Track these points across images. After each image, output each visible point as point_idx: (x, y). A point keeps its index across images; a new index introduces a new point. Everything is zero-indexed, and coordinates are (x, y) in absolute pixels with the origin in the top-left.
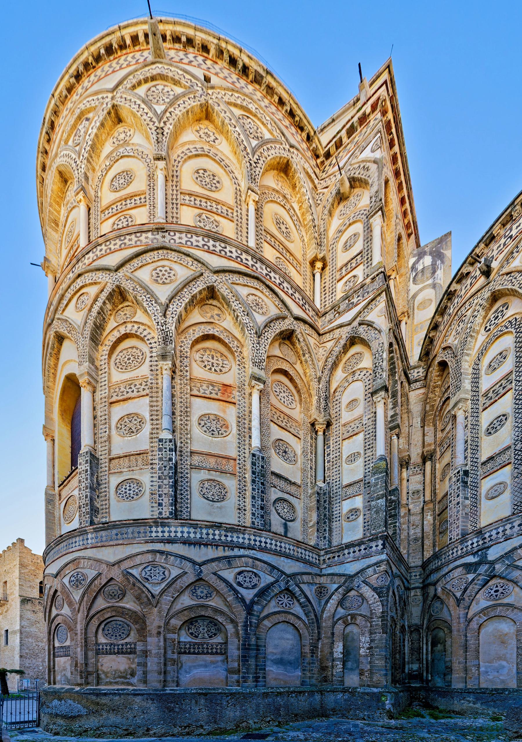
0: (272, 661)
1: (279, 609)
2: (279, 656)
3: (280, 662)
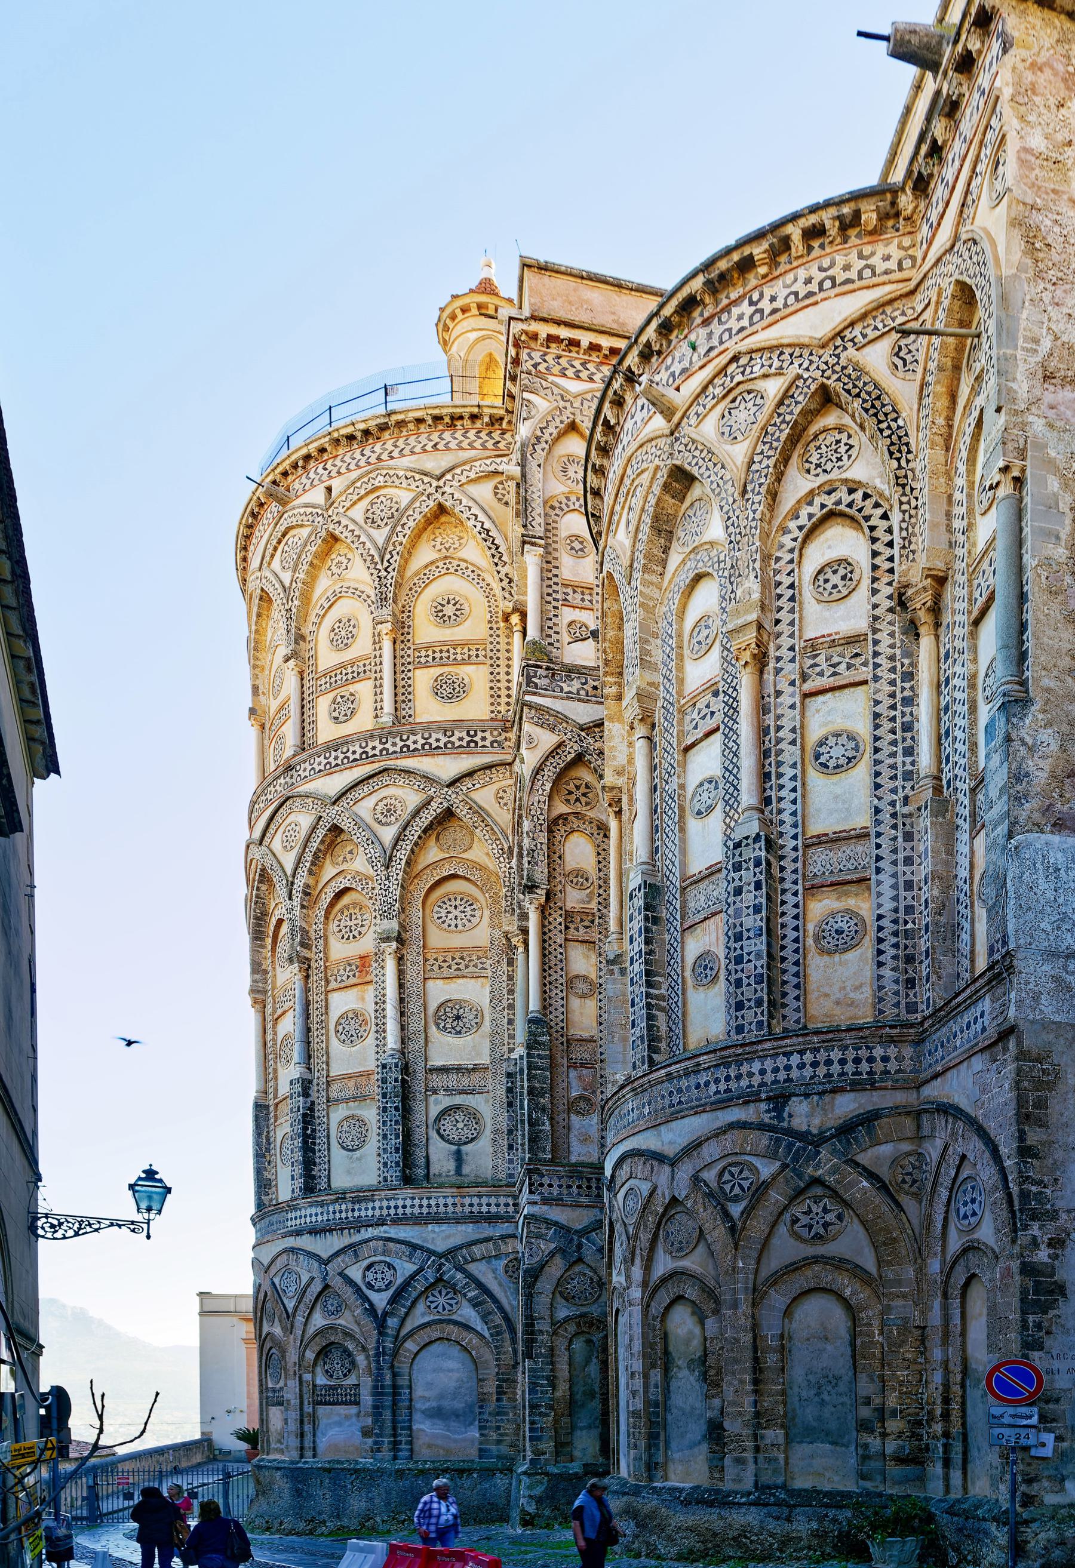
0: (423, 1412)
1: (432, 1318)
2: (434, 1404)
3: (437, 1413)
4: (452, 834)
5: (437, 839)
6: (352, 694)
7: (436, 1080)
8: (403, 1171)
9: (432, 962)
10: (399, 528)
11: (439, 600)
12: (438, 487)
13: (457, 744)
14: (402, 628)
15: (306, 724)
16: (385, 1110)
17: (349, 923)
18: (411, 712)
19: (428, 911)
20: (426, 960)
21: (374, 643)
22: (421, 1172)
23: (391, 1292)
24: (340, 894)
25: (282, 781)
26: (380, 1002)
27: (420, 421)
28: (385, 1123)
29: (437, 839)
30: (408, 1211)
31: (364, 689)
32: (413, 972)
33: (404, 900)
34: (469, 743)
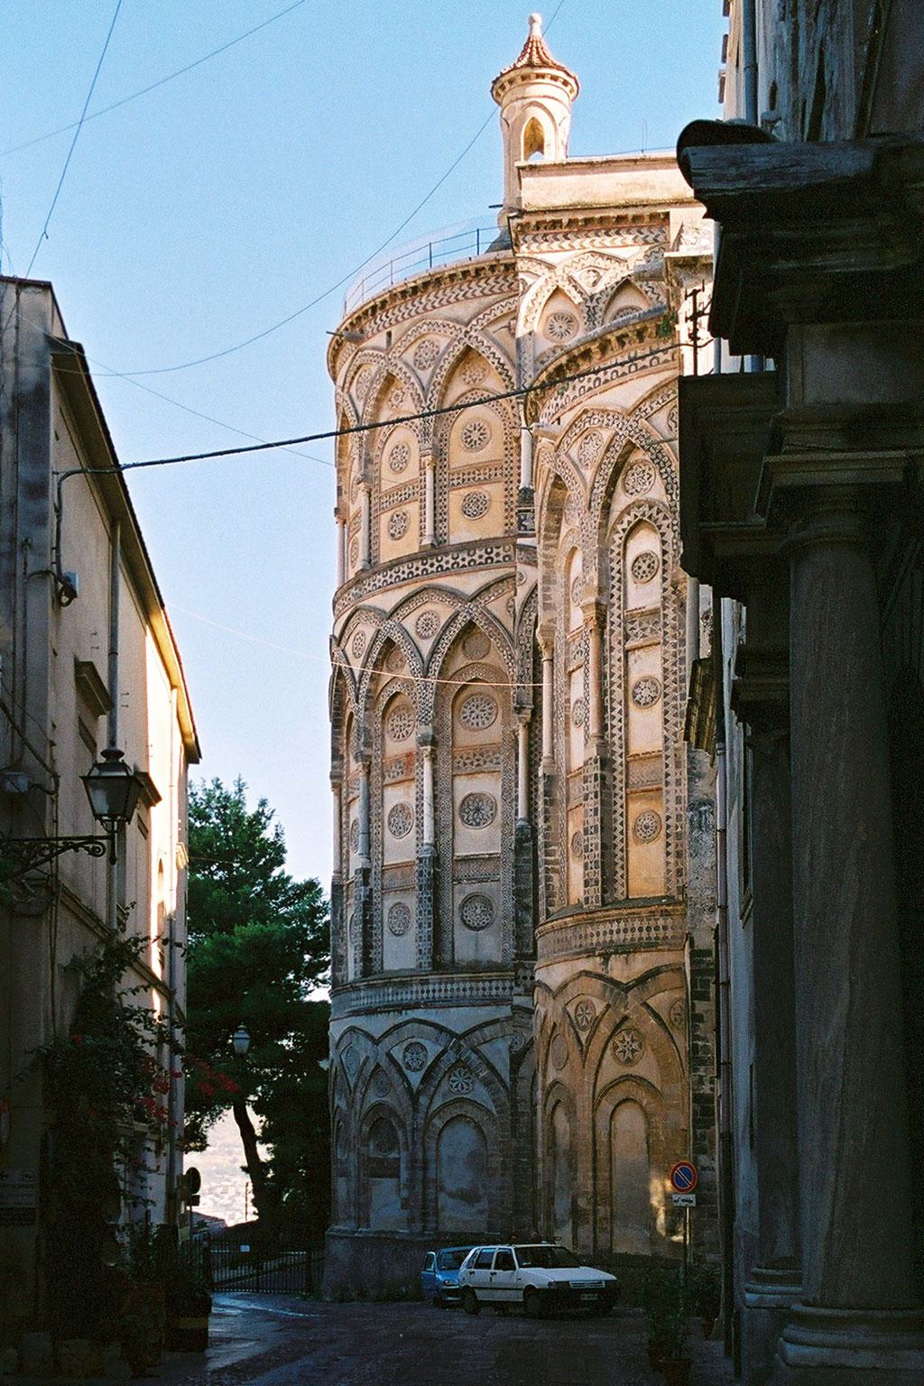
4: (473, 642)
5: (464, 647)
6: (404, 514)
7: (462, 870)
8: (433, 958)
9: (458, 759)
10: (438, 371)
11: (468, 427)
12: (467, 332)
13: (478, 561)
14: (439, 454)
15: (372, 538)
16: (421, 901)
17: (400, 723)
18: (446, 531)
19: (456, 712)
20: (454, 758)
21: (421, 469)
22: (447, 957)
23: (423, 1071)
24: (392, 698)
25: (353, 591)
26: (420, 798)
27: (452, 277)
28: (420, 912)
29: (464, 647)
30: (437, 995)
31: (412, 509)
32: (445, 769)
33: (438, 706)
34: (486, 559)
